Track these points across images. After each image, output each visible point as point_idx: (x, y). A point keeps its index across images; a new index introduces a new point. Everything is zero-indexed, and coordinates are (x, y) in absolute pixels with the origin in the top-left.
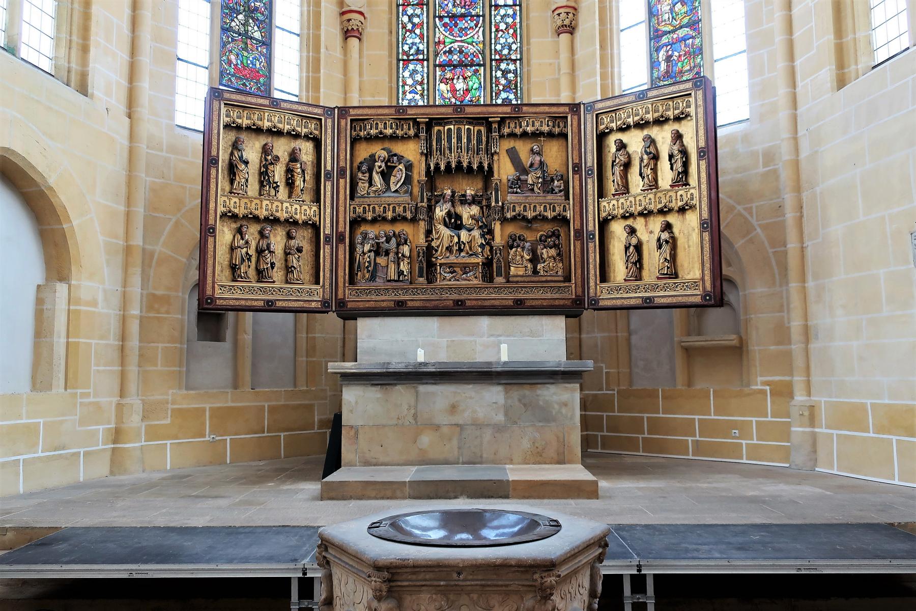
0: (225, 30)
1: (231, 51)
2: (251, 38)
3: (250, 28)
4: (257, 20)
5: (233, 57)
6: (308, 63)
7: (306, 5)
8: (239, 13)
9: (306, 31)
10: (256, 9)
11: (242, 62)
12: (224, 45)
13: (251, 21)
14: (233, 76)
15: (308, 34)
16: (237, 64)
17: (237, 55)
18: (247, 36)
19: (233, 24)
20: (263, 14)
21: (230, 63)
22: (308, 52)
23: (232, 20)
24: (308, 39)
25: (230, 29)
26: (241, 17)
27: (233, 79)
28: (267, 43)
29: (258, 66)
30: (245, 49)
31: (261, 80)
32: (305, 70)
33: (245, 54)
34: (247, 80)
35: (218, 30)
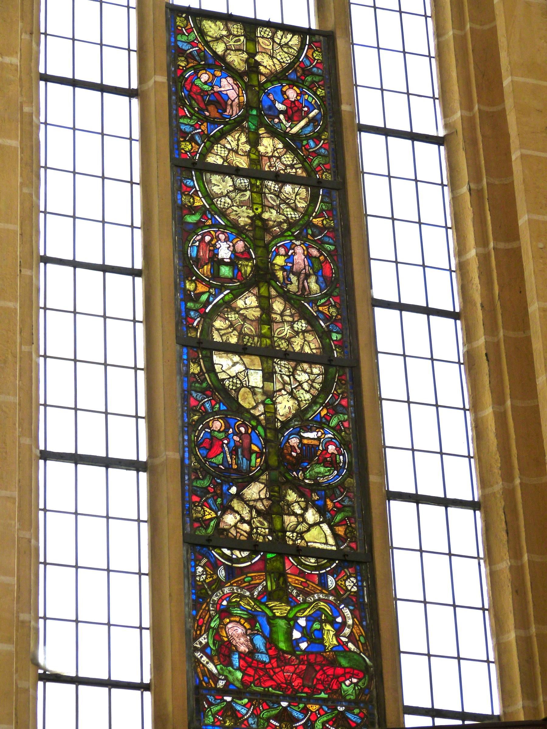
0: (201, 542)
1: (225, 613)
2: (300, 552)
3: (290, 521)
4: (316, 486)
5: (235, 631)
6: (519, 591)
7: (487, 398)
8: (246, 480)
9: (498, 487)
10: (309, 453)
11: (270, 642)
12: (200, 595)
13: (292, 496)
14: (238, 694)
15: (509, 494)
16: (254, 650)
17: (252, 619)
18: (280, 549)
19: (230, 519)
20: (332, 463)
21: (224, 651)
22: (516, 554)
23: (227, 508)
24: (510, 510)
25: (223, 538)
26: (254, 491)
27: (242, 707)
28: (363, 554)
29: (330, 639)
30: (281, 593)
31: (348, 686)
32: (510, 621)
33: (281, 609)
34: (294, 699)
35: (175, 550)
